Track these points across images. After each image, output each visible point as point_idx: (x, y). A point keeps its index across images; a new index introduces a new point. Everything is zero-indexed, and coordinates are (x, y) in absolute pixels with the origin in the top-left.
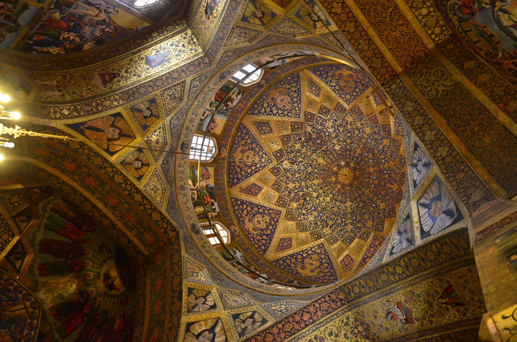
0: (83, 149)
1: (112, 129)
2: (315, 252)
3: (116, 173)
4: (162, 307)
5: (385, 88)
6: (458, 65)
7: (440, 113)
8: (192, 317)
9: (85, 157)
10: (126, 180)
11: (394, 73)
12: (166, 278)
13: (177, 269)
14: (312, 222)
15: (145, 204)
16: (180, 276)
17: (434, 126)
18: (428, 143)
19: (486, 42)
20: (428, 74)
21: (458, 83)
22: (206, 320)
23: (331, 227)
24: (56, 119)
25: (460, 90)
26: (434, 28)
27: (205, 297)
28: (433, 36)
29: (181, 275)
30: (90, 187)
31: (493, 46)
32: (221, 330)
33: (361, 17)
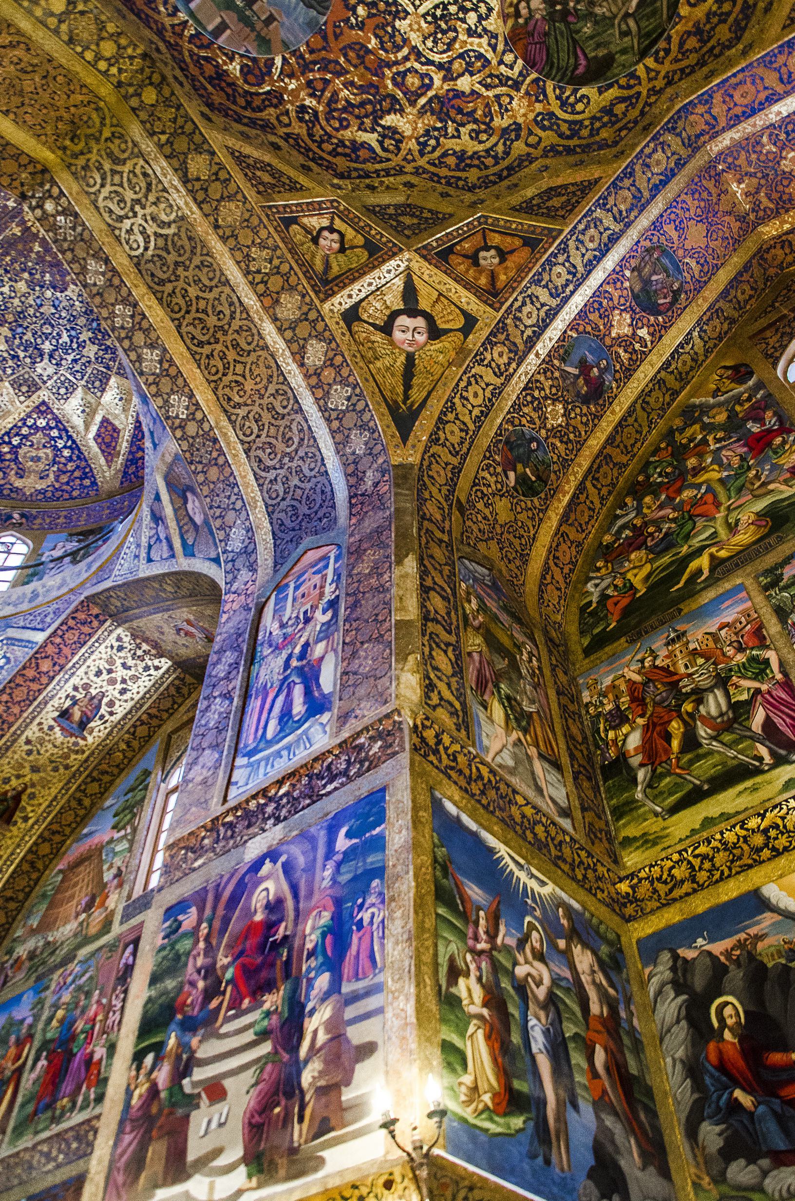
2: (36, 428)
5: (32, 209)
6: (175, 163)
7: (160, 300)
11: (39, 167)
14: (5, 355)
17: (153, 335)
18: (151, 379)
19: (241, 25)
20: (117, 179)
21: (183, 218)
23: (51, 356)
25: (190, 238)
26: (98, 45)
28: (102, 65)
31: (259, 36)
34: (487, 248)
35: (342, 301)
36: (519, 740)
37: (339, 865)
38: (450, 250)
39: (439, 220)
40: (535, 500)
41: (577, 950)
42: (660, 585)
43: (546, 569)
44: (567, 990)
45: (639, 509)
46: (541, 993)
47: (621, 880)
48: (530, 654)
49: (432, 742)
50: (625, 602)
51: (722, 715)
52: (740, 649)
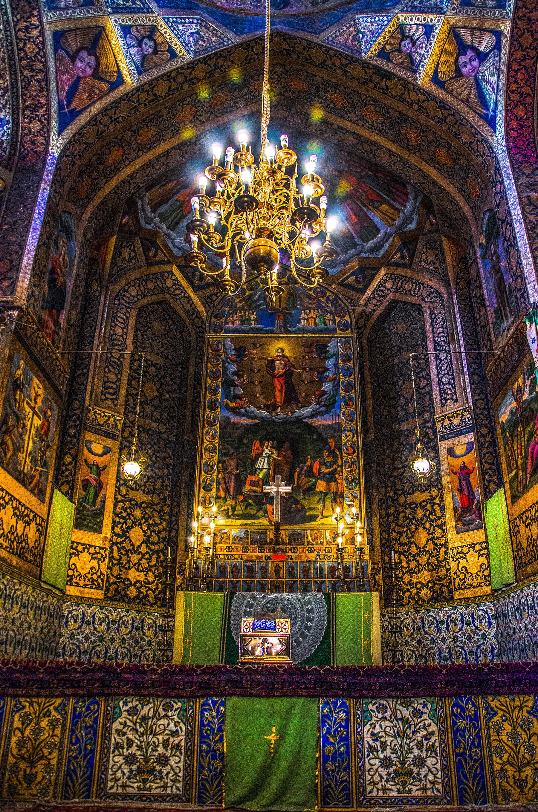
0: (101, 124)
1: (79, 64)
3: (152, 89)
4: (378, 109)
9: (112, 127)
10: (168, 76)
12: (338, 85)
13: (336, 61)
15: (215, 65)
16: (352, 60)
22: (444, 51)
24: (47, 145)
27: (404, 37)
29: (352, 58)
30: (152, 140)
32: (472, 34)
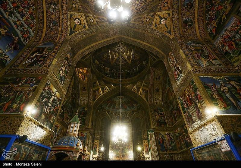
8: (139, 93)
33: (104, 40)
34: (165, 3)
35: (154, 25)
36: (208, 60)
37: (192, 89)
38: (161, 8)
39: (157, 6)
40: (192, 26)
41: (231, 82)
42: (219, 24)
43: (200, 33)
44: (231, 88)
45: (209, 15)
46: (227, 91)
47: (235, 68)
48: (204, 47)
49: (195, 71)
50: (215, 29)
51: (240, 38)
52: (238, 26)
